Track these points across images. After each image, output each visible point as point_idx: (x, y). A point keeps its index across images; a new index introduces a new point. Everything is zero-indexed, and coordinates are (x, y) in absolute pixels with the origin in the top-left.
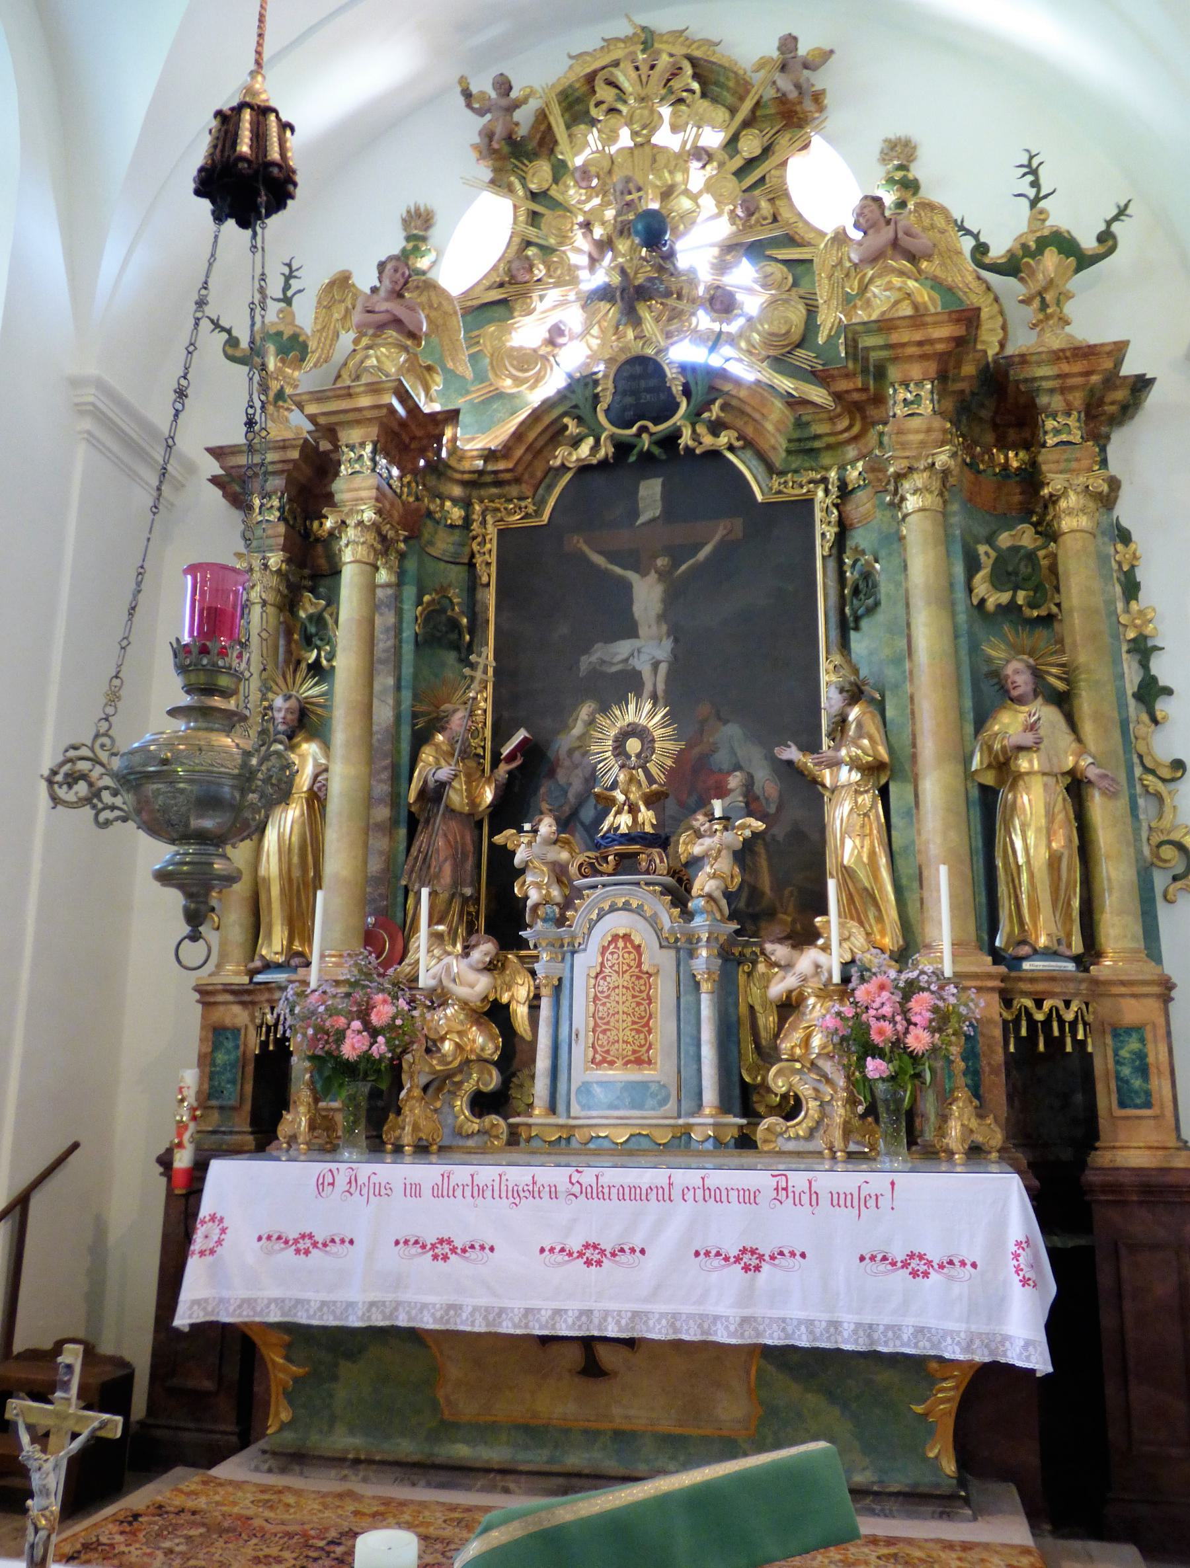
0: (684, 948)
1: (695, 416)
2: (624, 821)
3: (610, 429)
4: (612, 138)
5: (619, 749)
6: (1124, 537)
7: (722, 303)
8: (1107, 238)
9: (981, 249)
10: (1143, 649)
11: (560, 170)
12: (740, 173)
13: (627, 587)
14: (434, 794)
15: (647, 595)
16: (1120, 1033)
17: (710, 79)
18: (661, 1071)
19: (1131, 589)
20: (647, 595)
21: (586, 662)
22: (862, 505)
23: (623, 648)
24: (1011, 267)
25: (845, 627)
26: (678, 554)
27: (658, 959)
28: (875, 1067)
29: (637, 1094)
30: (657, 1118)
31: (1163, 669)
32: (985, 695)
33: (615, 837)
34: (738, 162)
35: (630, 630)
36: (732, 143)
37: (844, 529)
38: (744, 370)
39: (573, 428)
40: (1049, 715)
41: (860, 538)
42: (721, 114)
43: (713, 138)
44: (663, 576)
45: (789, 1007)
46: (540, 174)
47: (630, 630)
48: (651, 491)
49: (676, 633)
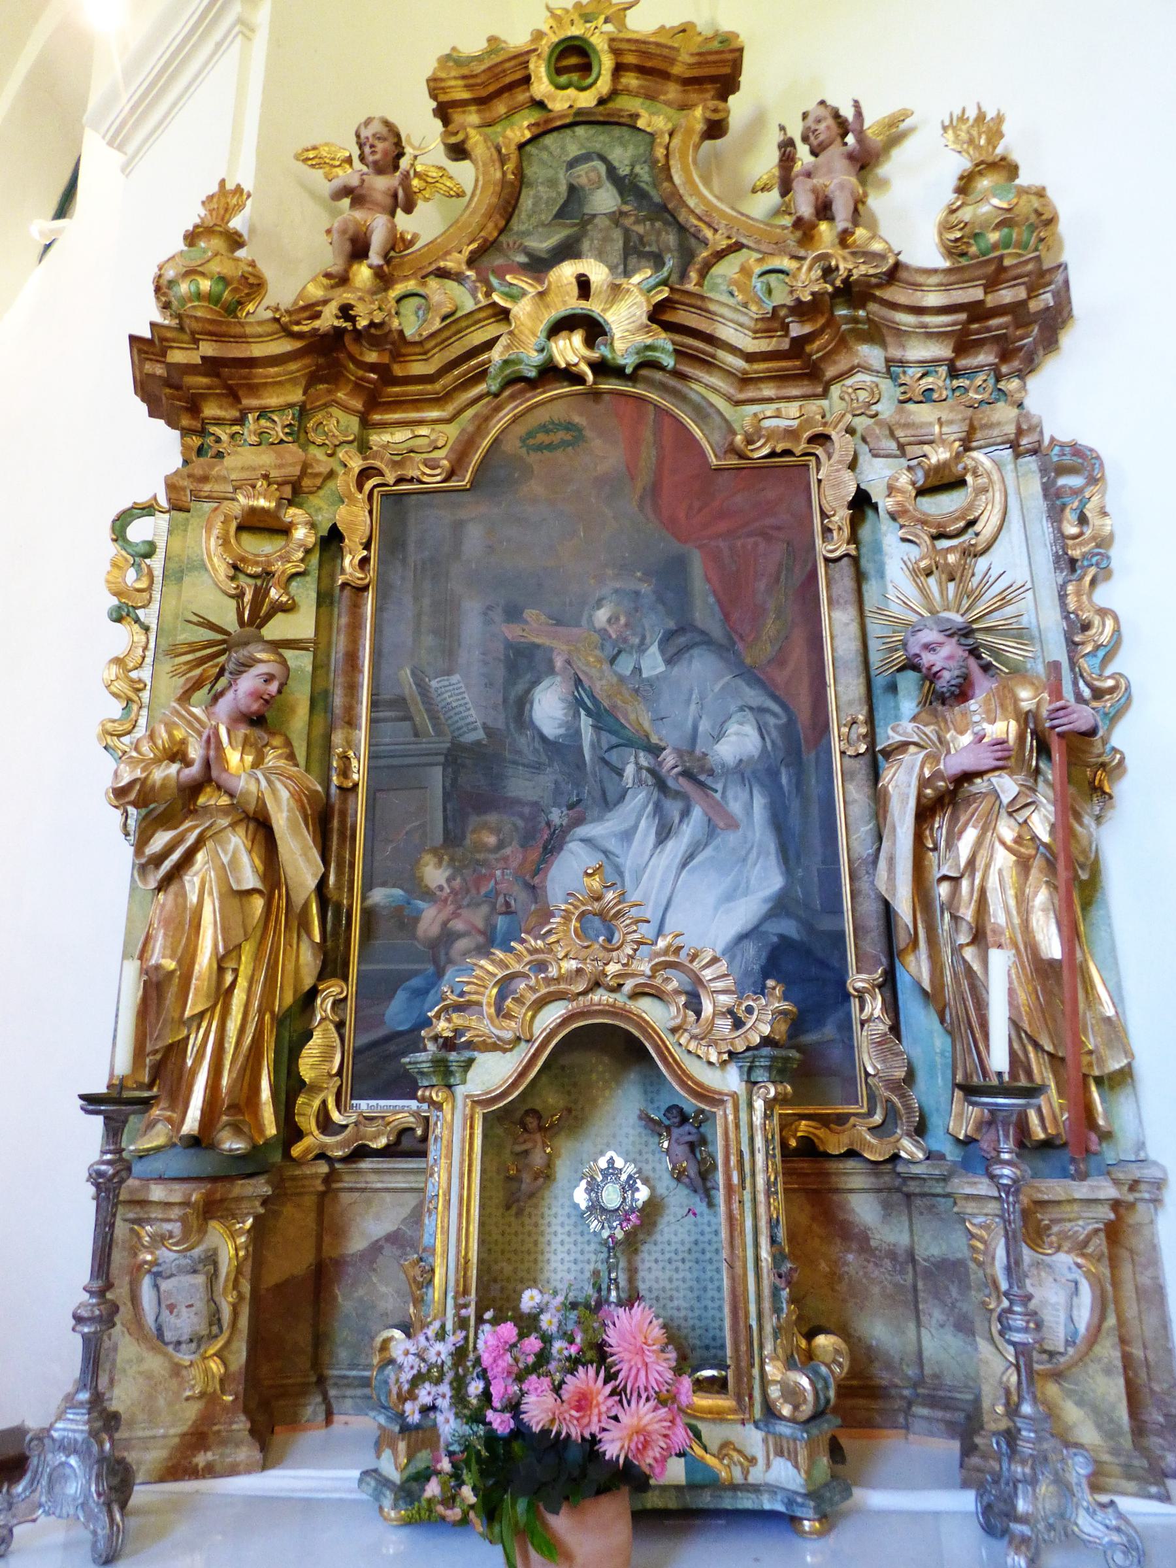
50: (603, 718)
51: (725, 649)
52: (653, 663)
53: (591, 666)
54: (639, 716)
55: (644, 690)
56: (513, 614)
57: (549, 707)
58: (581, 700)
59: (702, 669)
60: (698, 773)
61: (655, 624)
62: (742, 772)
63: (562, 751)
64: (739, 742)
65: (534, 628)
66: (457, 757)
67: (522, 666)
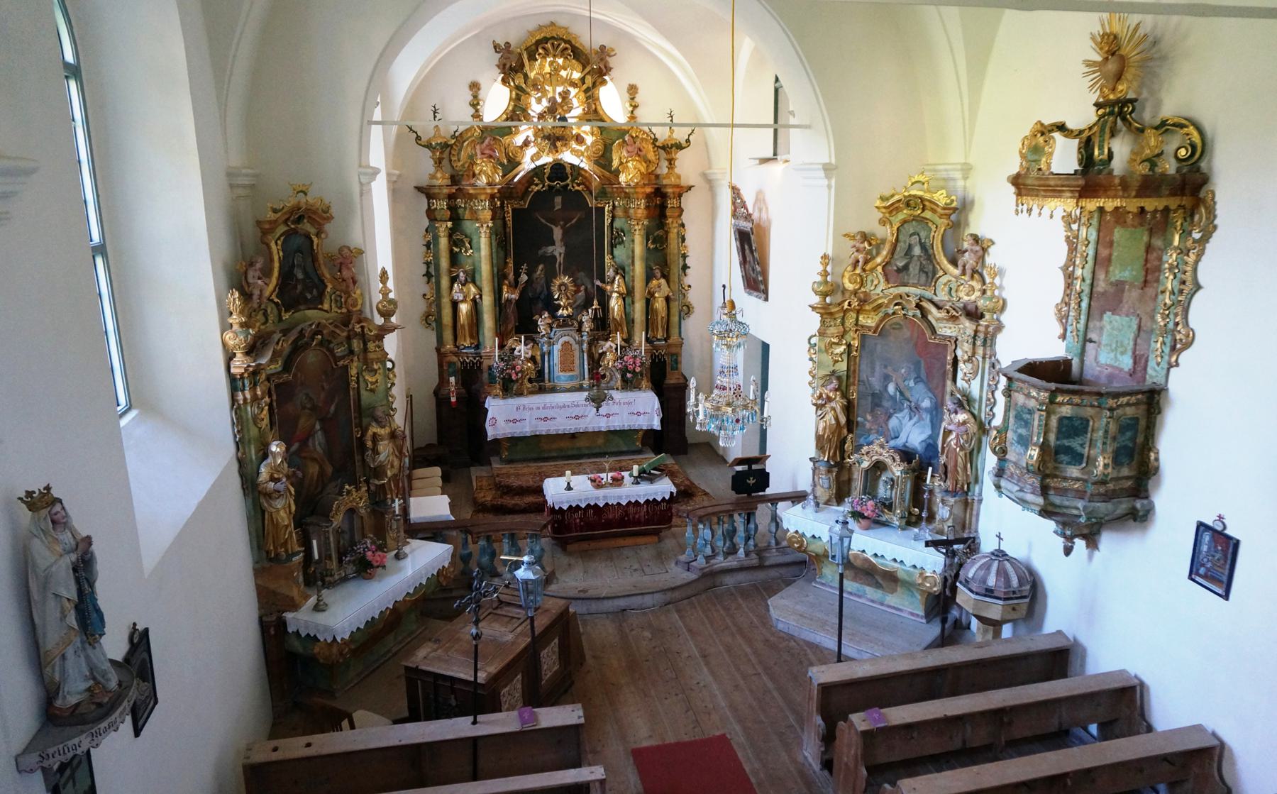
0: (580, 343)
1: (573, 181)
2: (565, 313)
3: (547, 183)
4: (542, 67)
5: (560, 290)
6: (683, 225)
7: (579, 139)
8: (688, 141)
9: (656, 140)
10: (684, 256)
11: (526, 77)
12: (586, 91)
13: (552, 231)
14: (508, 301)
15: (558, 233)
16: (672, 355)
17: (577, 53)
18: (576, 373)
19: (683, 240)
20: (558, 233)
21: (540, 252)
22: (619, 212)
23: (550, 249)
24: (664, 148)
25: (612, 246)
26: (567, 220)
27: (576, 347)
28: (629, 375)
29: (571, 378)
30: (576, 383)
31: (688, 261)
32: (649, 277)
33: (562, 316)
34: (585, 87)
35: (553, 244)
36: (583, 80)
37: (613, 218)
38: (585, 165)
39: (536, 181)
40: (663, 281)
41: (617, 224)
42: (580, 67)
43: (576, 75)
44: (562, 228)
45: (604, 353)
46: (520, 80)
47: (553, 244)
48: (558, 200)
49: (566, 245)
50: (901, 393)
51: (927, 384)
52: (912, 383)
53: (900, 381)
54: (908, 394)
55: (910, 389)
56: (886, 367)
57: (891, 388)
58: (897, 388)
59: (921, 386)
60: (918, 408)
61: (913, 375)
62: (926, 410)
63: (893, 398)
64: (926, 404)
65: (889, 371)
66: (873, 395)
67: (887, 378)
